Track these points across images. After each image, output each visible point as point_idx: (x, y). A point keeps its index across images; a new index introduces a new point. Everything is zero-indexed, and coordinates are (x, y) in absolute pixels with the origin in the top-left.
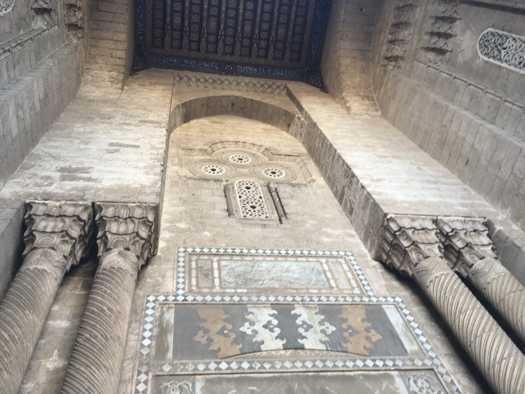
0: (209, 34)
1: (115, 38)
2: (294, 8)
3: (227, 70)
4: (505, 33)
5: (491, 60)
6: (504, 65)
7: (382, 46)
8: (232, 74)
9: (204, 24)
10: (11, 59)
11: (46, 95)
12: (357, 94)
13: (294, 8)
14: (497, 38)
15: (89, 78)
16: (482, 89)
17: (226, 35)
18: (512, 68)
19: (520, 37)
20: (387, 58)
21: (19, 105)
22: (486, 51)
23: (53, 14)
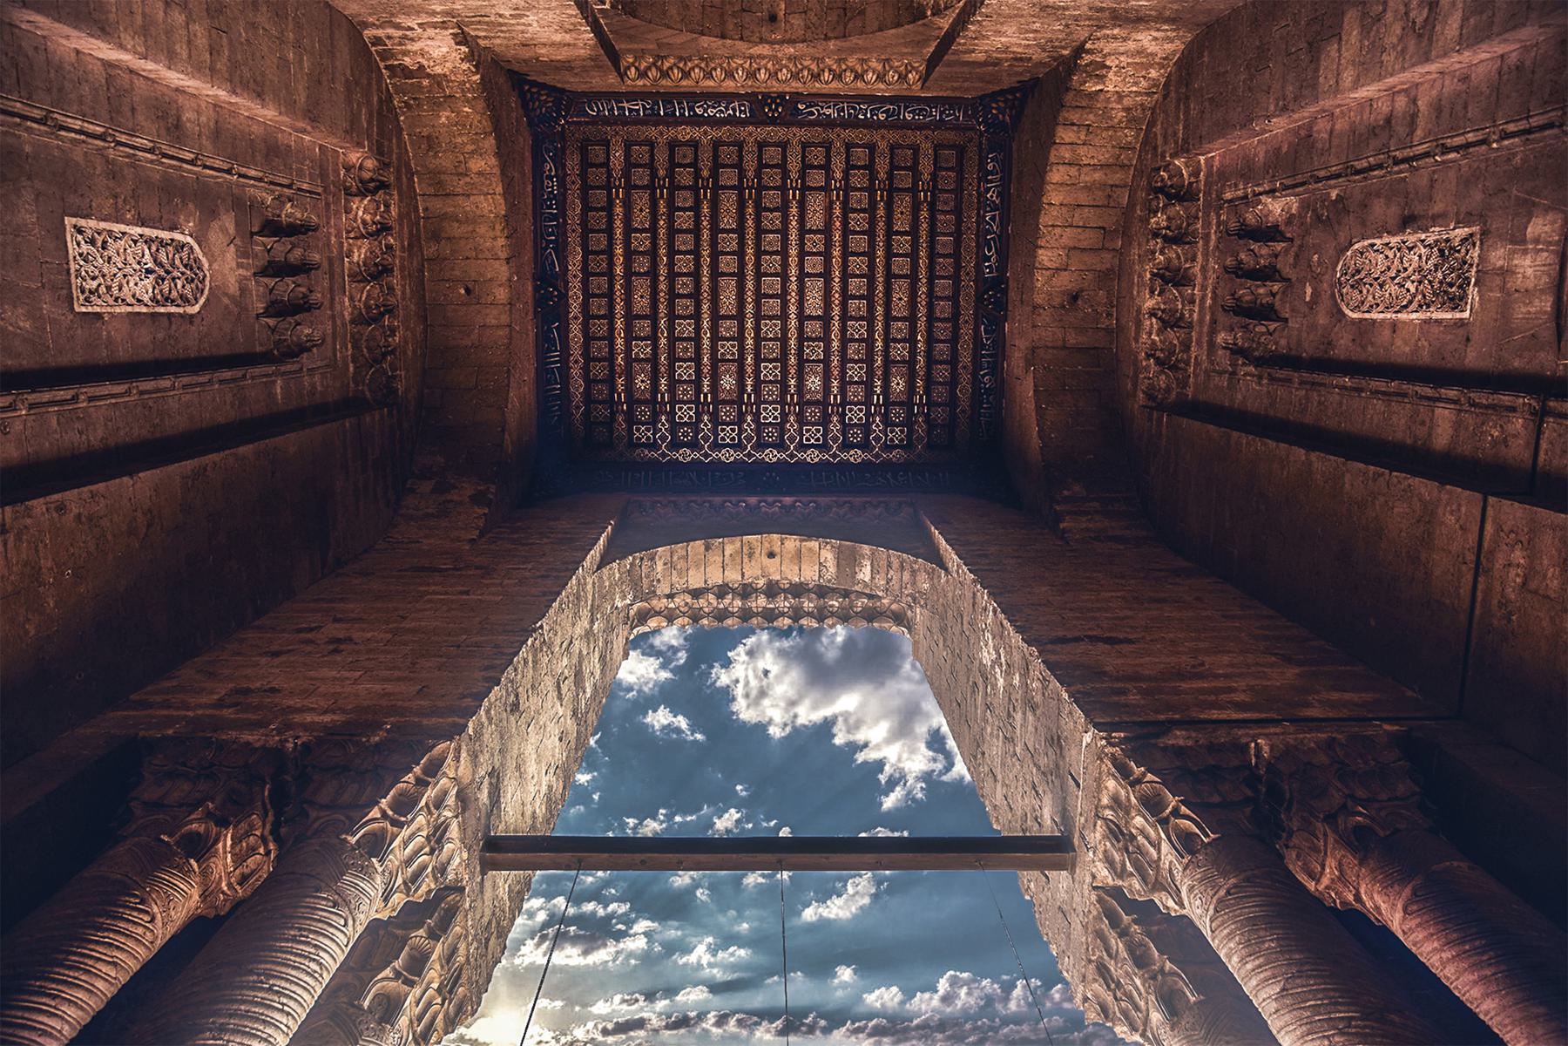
0: (826, 189)
1: (1073, 171)
2: (619, 270)
3: (777, 105)
4: (162, 310)
5: (165, 235)
6: (136, 231)
7: (399, 214)
8: (766, 95)
9: (837, 212)
10: (1393, 142)
11: (1314, 50)
12: (438, 80)
13: (619, 270)
14: (174, 294)
15: (1153, 73)
16: (165, 156)
17: (783, 189)
18: (118, 228)
19: (129, 309)
20: (383, 186)
21: (1420, 36)
22: (184, 254)
23: (1233, 225)
